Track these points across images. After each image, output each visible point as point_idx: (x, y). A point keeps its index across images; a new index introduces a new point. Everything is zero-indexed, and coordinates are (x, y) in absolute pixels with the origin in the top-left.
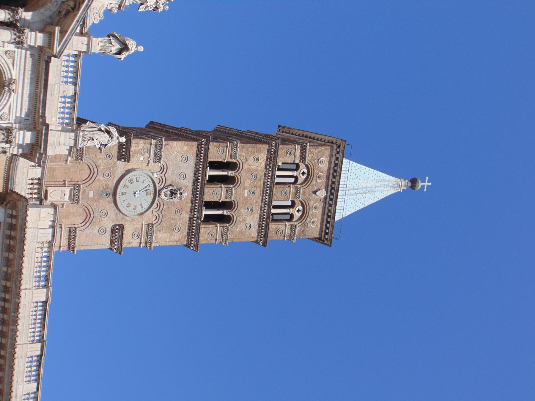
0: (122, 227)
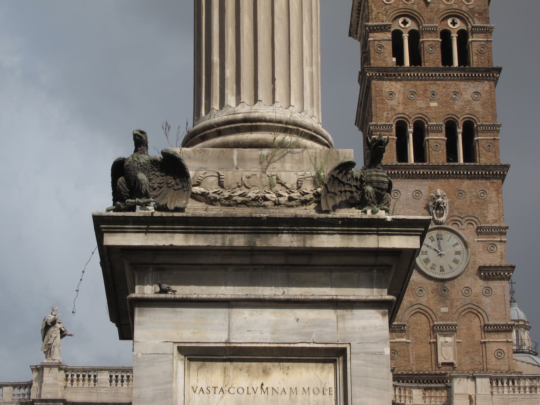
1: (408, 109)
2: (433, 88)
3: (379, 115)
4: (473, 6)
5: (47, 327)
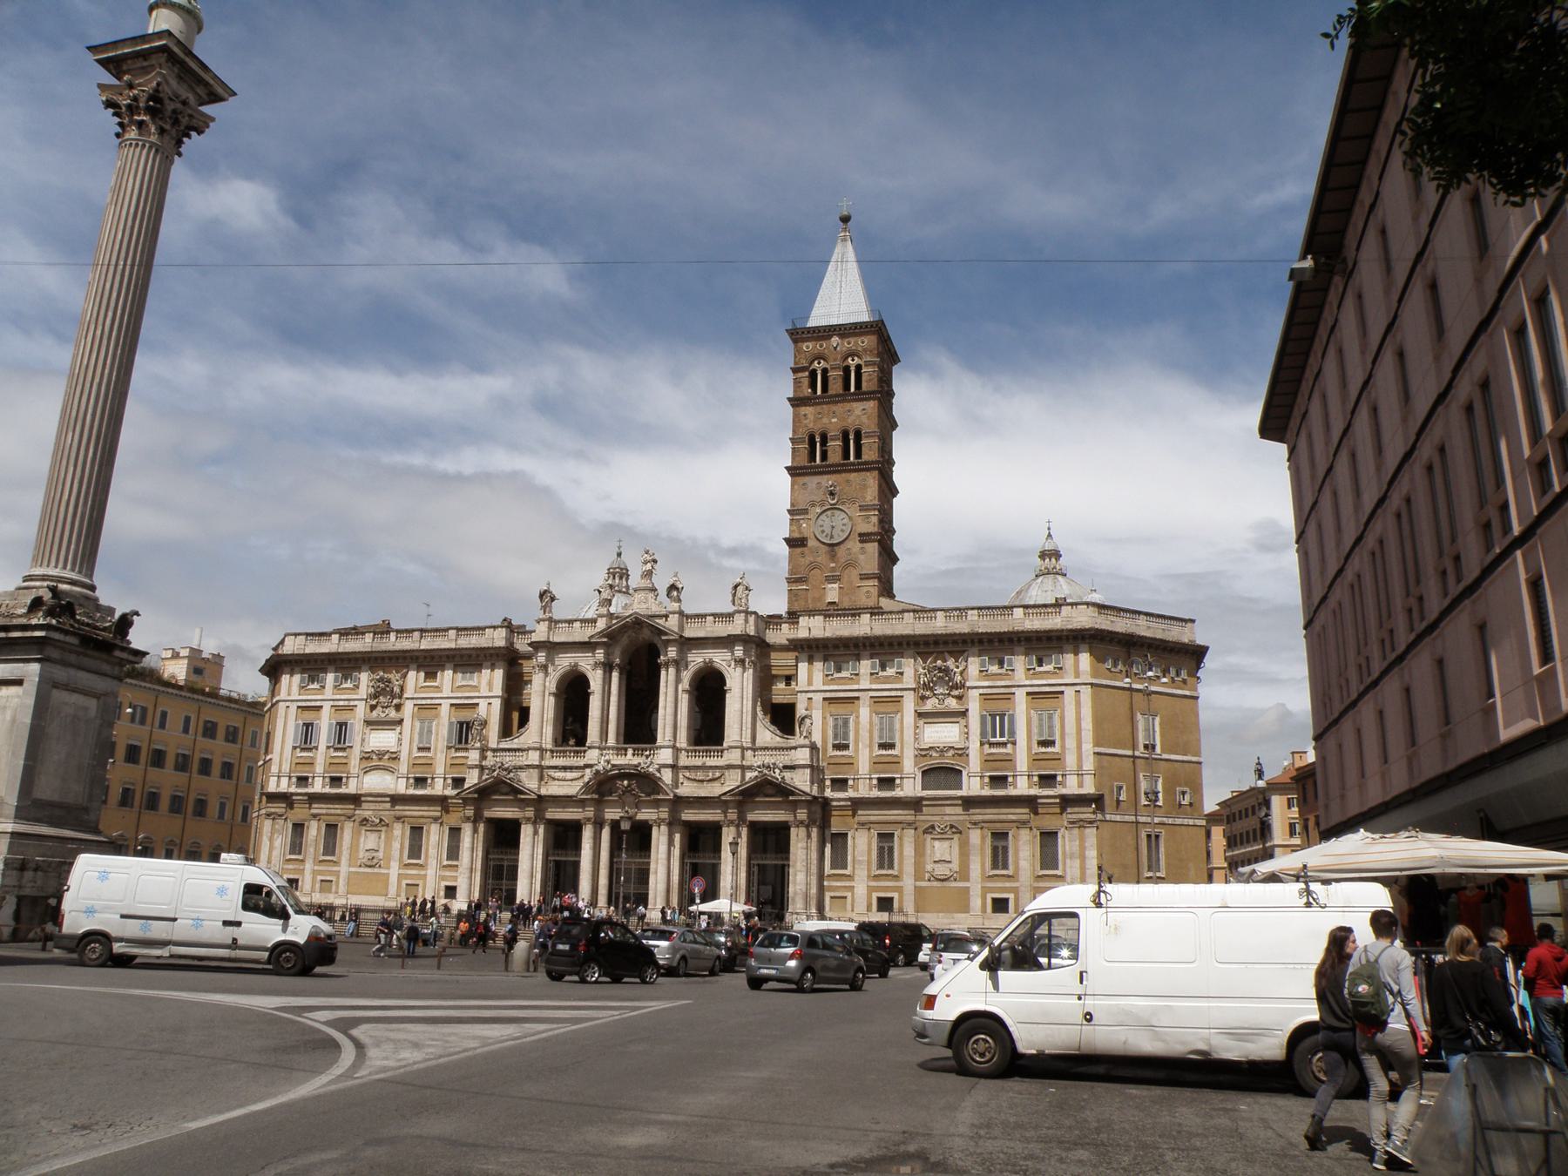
0: (860, 535)
5: (542, 596)
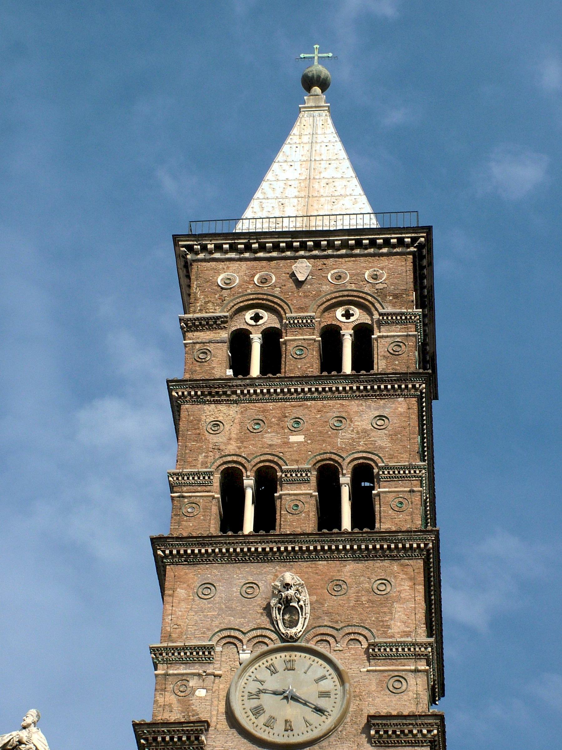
1: (245, 447)
2: (298, 412)
3: (190, 459)
4: (386, 286)
